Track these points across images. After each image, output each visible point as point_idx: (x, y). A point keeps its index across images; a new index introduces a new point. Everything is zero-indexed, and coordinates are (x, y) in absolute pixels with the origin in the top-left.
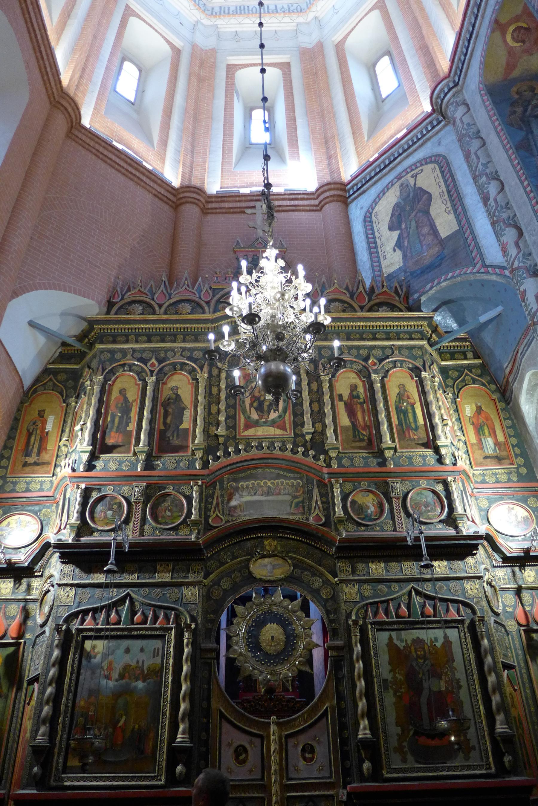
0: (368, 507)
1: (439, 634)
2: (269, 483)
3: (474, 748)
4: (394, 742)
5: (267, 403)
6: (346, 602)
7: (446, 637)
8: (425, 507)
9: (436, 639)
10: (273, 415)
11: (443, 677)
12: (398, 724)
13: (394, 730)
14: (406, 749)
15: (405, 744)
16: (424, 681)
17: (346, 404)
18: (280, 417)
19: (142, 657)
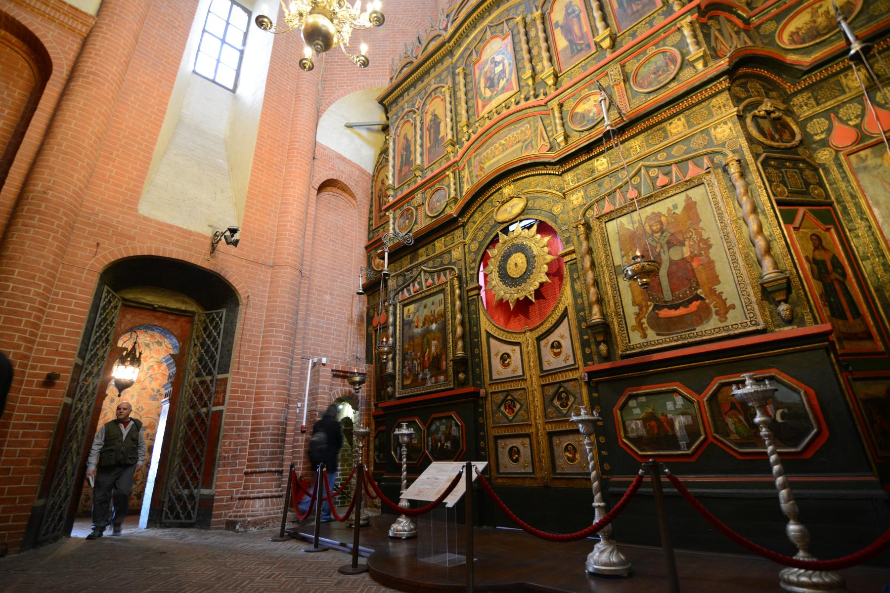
0: (590, 111)
1: (680, 200)
2: (503, 142)
3: (733, 307)
4: (631, 321)
5: (496, 77)
6: (573, 209)
7: (688, 198)
8: (655, 73)
9: (675, 207)
10: (502, 83)
11: (687, 243)
12: (634, 303)
13: (631, 311)
14: (646, 325)
15: (644, 320)
16: (662, 254)
17: (562, 27)
18: (507, 81)
19: (433, 308)
